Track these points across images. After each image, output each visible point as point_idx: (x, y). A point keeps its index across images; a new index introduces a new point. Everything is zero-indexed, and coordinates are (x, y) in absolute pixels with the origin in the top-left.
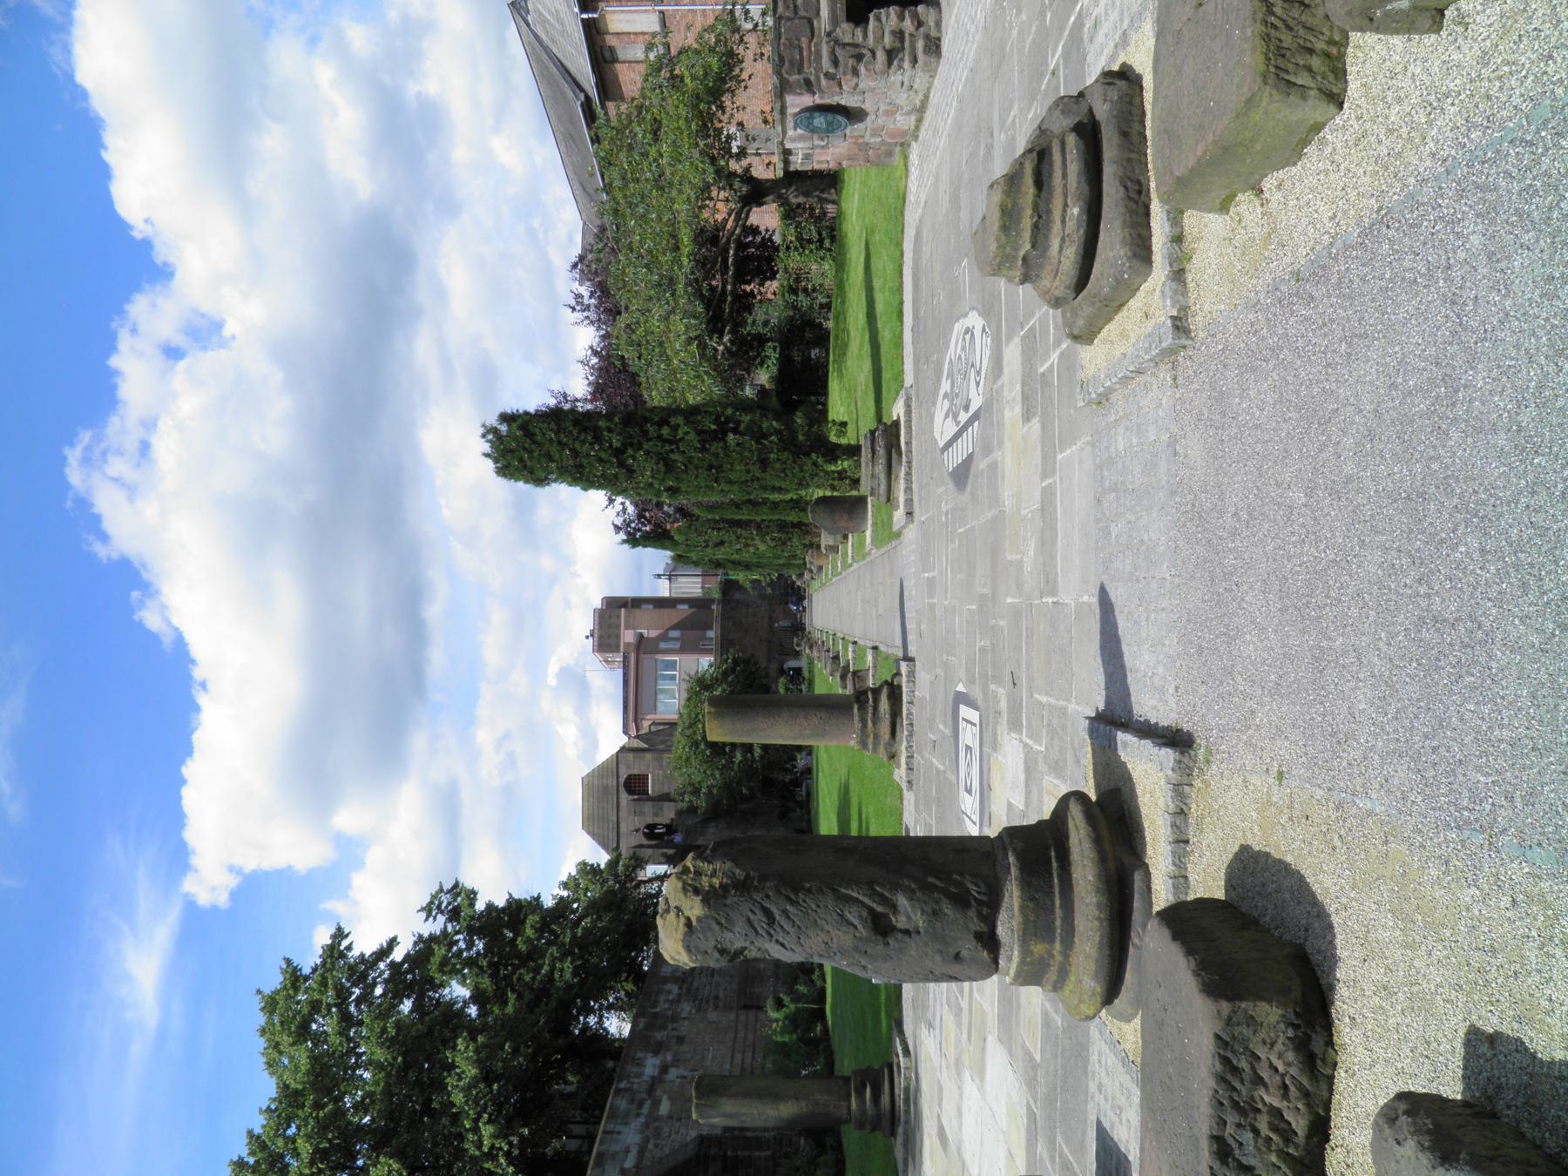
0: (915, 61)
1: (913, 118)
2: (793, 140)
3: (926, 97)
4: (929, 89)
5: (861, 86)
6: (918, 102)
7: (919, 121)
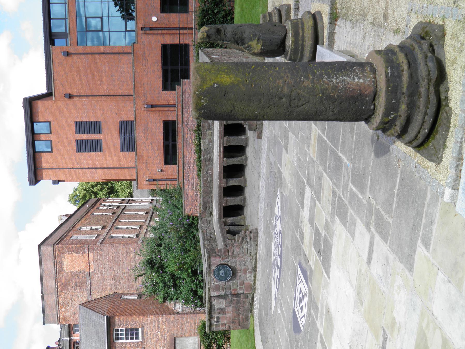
0: (251, 239)
1: (253, 275)
2: (213, 291)
3: (256, 260)
5: (235, 253)
6: (253, 264)
7: (255, 277)
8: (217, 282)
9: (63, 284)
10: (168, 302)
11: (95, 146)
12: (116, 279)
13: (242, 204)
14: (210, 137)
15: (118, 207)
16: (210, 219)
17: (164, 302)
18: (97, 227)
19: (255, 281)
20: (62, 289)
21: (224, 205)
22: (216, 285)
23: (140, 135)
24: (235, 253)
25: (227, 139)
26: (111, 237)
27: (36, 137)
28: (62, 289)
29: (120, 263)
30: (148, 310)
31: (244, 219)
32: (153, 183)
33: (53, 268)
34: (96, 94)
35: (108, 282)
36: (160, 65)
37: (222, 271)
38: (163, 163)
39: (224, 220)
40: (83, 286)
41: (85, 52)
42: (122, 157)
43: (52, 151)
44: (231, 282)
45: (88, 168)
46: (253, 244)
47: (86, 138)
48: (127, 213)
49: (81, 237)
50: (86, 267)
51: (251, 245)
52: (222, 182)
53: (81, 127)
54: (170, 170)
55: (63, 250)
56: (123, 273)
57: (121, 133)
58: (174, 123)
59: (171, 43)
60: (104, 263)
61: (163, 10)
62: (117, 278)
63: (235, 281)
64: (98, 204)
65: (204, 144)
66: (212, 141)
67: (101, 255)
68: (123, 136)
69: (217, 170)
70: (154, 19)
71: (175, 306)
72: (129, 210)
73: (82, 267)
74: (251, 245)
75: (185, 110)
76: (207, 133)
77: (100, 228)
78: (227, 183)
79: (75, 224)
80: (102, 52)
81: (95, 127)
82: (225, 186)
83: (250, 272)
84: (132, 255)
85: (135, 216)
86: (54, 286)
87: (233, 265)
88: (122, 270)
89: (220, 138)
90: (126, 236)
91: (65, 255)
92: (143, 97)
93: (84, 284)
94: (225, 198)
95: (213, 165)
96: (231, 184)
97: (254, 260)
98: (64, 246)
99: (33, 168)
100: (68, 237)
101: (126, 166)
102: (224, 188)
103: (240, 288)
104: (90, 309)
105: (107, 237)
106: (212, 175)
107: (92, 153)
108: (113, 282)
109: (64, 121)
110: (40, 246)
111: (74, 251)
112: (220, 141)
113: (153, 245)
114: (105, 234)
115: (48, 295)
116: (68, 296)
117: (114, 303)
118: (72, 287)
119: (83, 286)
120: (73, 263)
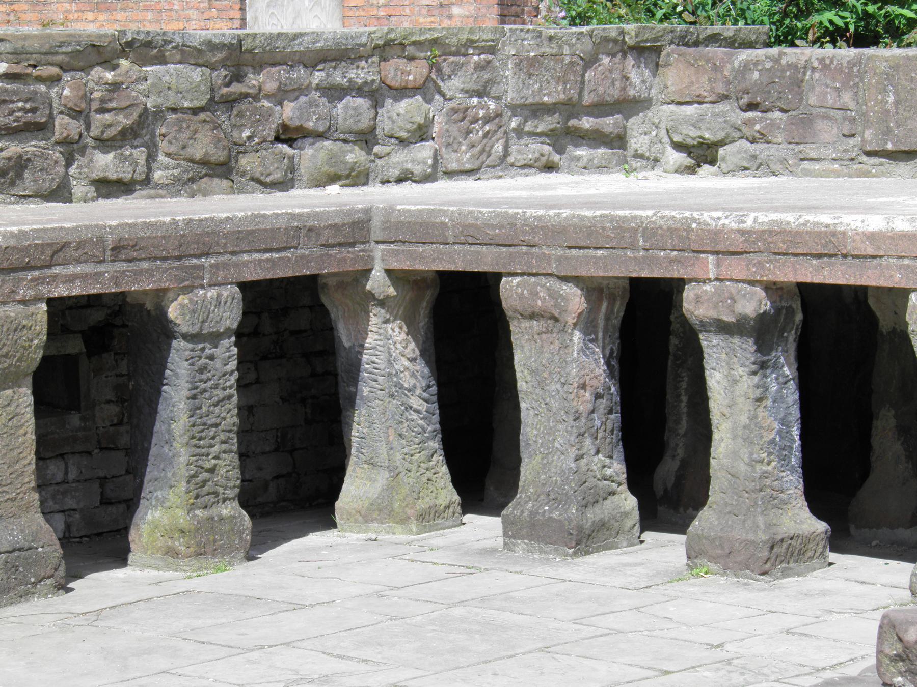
13: (524, 503)
16: (638, 142)
21: (511, 291)
31: (380, 512)
39: (378, 282)
52: (736, 268)
78: (724, 328)
82: (696, 304)
94: (575, 300)
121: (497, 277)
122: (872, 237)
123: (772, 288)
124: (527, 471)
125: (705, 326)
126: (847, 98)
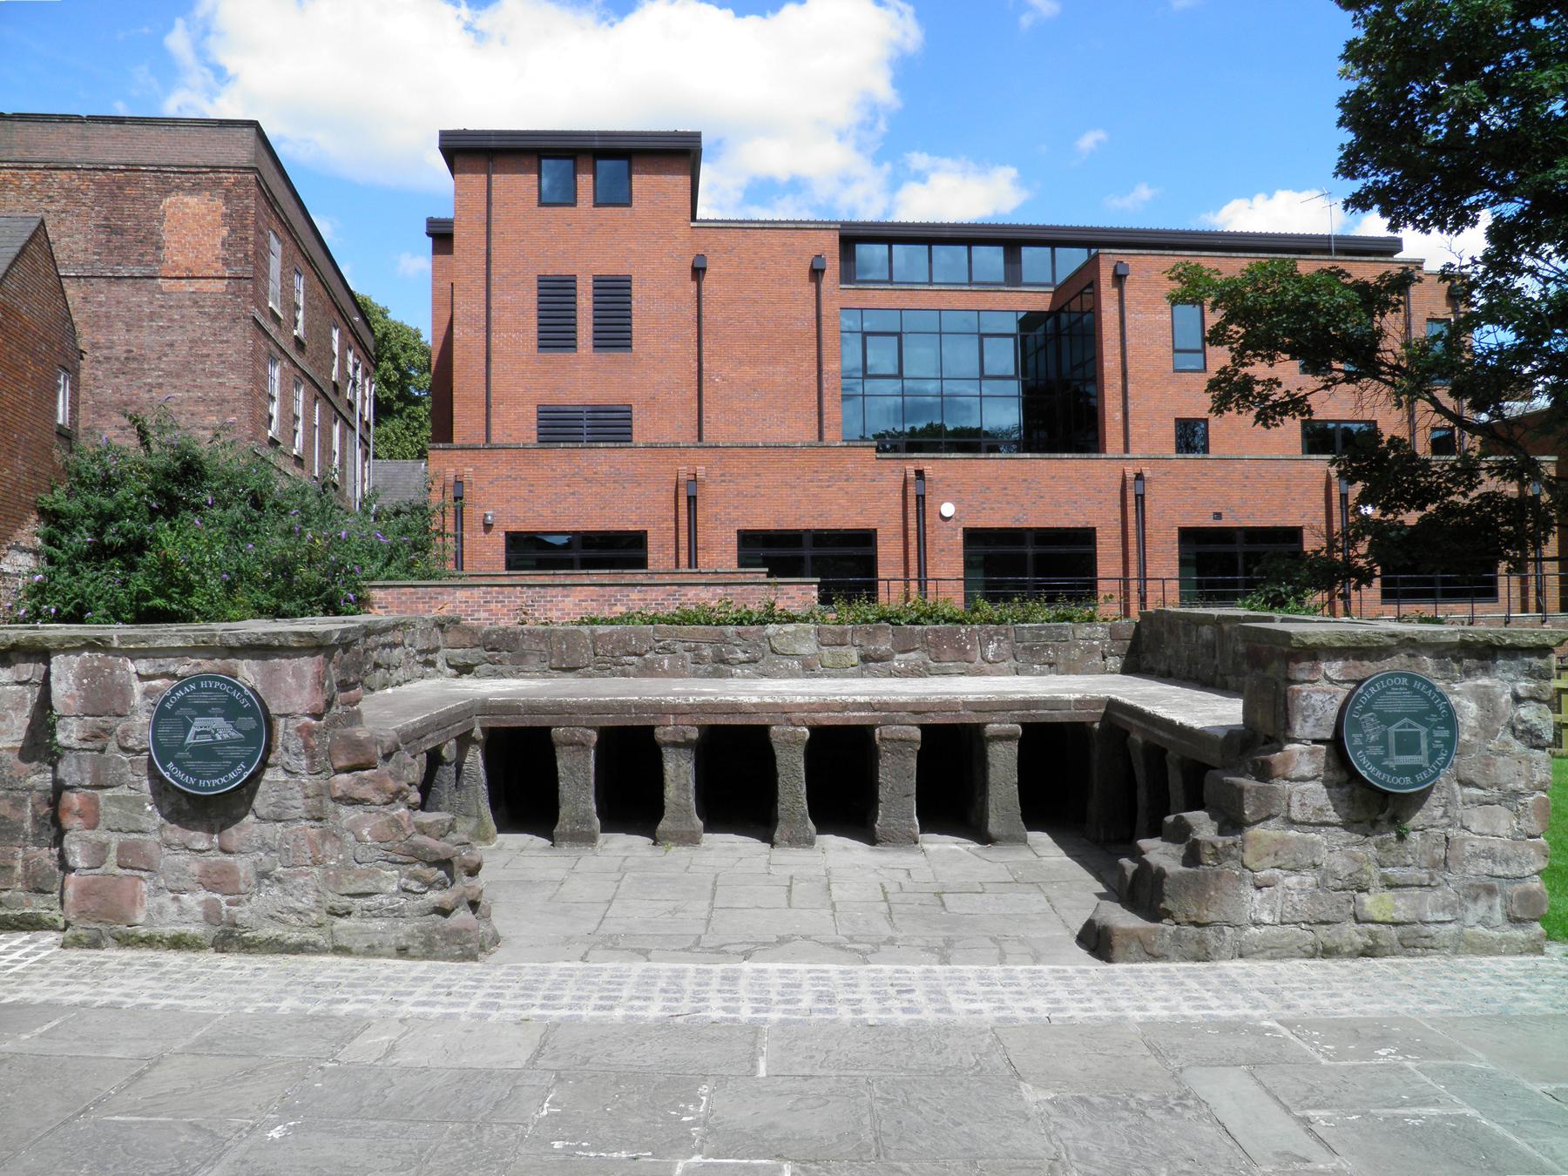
0: (444, 912)
1: (194, 930)
3: (299, 949)
4: (340, 950)
5: (348, 814)
6: (269, 931)
7: (178, 943)
8: (147, 693)
9: (120, 188)
10: (42, 528)
11: (555, 332)
12: (131, 363)
14: (828, 662)
15: (351, 405)
16: (439, 665)
17: (42, 513)
18: (300, 324)
19: (149, 942)
20: (100, 185)
21: (558, 733)
22: (124, 692)
23: (602, 459)
24: (344, 810)
25: (912, 741)
26: (274, 361)
27: (585, 162)
28: (100, 185)
29: (187, 379)
30: (12, 454)
32: (450, 494)
33: (176, 162)
34: (705, 346)
35: (120, 335)
36: (816, 525)
37: (221, 728)
38: (513, 528)
40: (111, 253)
41: (824, 319)
42: (520, 410)
43: (541, 204)
44: (146, 785)
45: (488, 308)
46: (406, 927)
47: (579, 307)
48: (336, 430)
49: (275, 265)
50: (177, 267)
51: (398, 913)
52: (685, 720)
53: (614, 295)
54: (489, 551)
55: (239, 197)
56: (151, 387)
57: (595, 409)
58: (641, 563)
59: (880, 558)
60: (189, 327)
61: (973, 537)
62: (134, 365)
63: (151, 816)
64: (359, 351)
65: (794, 634)
66: (809, 669)
67: (214, 319)
68: (585, 415)
69: (748, 691)
70: (948, 509)
71: (24, 550)
72: (343, 437)
73: (176, 254)
74: (398, 913)
75: (719, 590)
76: (843, 650)
77: (299, 331)
78: (675, 745)
79: (309, 261)
80: (825, 368)
81: (615, 332)
82: (659, 734)
83: (211, 914)
84: (214, 420)
85: (327, 450)
86: (113, 160)
87: (262, 801)
88: (160, 385)
89: (918, 703)
90: (274, 409)
91: (219, 202)
92: (717, 472)
93: (115, 258)
95: (695, 675)
96: (669, 767)
97: (295, 937)
98: (250, 202)
99: (493, 144)
100: (275, 225)
101: (493, 420)
102: (652, 728)
103: (103, 848)
104: (23, 250)
105: (273, 348)
106: (648, 670)
107: (534, 321)
108: (119, 351)
109: (633, 246)
110: (254, 124)
111: (233, 230)
112: (903, 706)
113: (253, 483)
114: (281, 341)
115: (83, 137)
116: (77, 202)
117: (42, 339)
118: (106, 218)
119: (111, 253)
120: (194, 226)
121: (548, 729)
122: (754, 705)
123: (700, 727)
124: (563, 811)
125: (666, 744)
126: (542, 646)
